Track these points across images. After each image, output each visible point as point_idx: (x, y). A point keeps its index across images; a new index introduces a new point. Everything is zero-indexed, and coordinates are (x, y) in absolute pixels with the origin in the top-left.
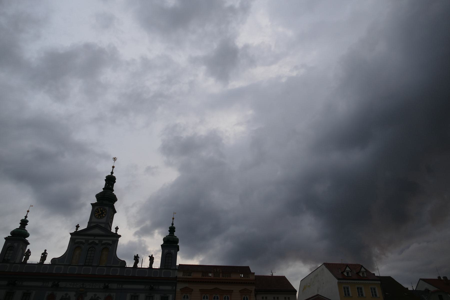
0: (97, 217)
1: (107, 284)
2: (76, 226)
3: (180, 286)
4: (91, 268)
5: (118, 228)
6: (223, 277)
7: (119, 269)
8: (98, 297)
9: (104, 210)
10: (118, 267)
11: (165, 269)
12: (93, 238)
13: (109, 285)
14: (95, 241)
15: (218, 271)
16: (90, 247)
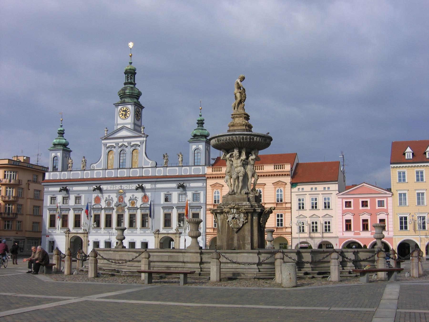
0: (122, 117)
3: (210, 182)
4: (125, 170)
7: (150, 169)
8: (136, 197)
9: (128, 109)
11: (194, 166)
12: (121, 140)
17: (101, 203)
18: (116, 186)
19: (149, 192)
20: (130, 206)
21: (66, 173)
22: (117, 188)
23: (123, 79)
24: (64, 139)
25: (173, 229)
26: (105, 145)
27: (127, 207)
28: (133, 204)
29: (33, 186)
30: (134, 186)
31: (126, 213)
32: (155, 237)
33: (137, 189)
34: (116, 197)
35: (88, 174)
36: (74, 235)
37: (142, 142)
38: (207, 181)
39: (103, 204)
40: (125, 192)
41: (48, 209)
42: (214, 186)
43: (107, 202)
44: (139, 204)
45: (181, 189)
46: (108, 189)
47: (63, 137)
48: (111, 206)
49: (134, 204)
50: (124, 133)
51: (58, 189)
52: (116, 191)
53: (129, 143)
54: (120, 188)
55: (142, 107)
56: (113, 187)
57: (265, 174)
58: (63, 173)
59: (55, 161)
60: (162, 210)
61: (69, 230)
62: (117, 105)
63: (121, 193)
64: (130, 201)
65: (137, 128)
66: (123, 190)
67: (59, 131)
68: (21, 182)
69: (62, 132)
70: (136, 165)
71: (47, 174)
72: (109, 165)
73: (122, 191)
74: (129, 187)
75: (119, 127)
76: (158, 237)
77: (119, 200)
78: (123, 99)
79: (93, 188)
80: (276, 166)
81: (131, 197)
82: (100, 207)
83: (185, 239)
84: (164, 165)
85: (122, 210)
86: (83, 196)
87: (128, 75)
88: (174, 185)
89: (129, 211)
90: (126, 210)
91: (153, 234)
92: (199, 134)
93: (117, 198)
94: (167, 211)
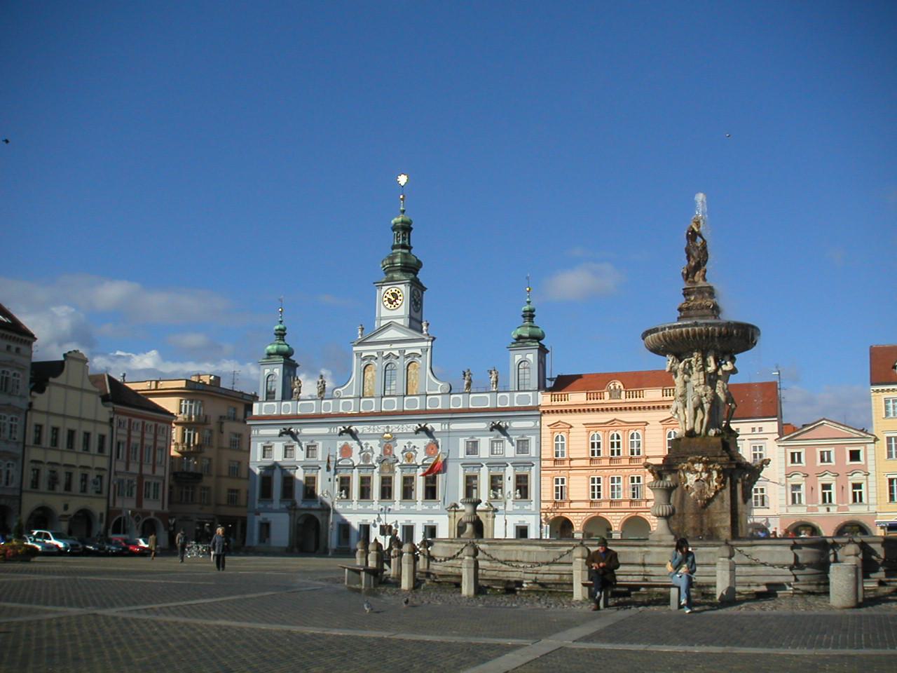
1: (423, 425)
3: (548, 420)
4: (395, 399)
6: (628, 398)
7: (439, 397)
8: (415, 447)
10: (439, 394)
11: (519, 391)
12: (388, 346)
14: (393, 352)
15: (617, 387)
16: (387, 365)
17: (351, 456)
18: (379, 426)
20: (404, 463)
21: (289, 403)
22: (381, 431)
23: (392, 238)
24: (286, 344)
26: (359, 354)
27: (399, 464)
28: (409, 458)
29: (230, 427)
30: (413, 427)
31: (396, 474)
32: (450, 517)
33: (417, 432)
34: (380, 446)
35: (328, 406)
36: (303, 513)
37: (424, 350)
38: (542, 418)
39: (356, 459)
40: (394, 438)
41: (259, 467)
42: (554, 425)
43: (364, 455)
44: (420, 458)
45: (496, 432)
46: (365, 432)
47: (284, 340)
50: (391, 334)
51: (277, 431)
52: (379, 437)
53: (402, 351)
54: (386, 430)
55: (424, 289)
57: (647, 405)
58: (284, 403)
59: (269, 383)
60: (461, 469)
61: (294, 504)
62: (380, 284)
63: (389, 438)
64: (404, 454)
65: (414, 323)
66: (391, 434)
67: (277, 330)
68: (208, 419)
69: (282, 332)
70: (414, 390)
71: (256, 406)
72: (367, 390)
73: (389, 435)
75: (383, 323)
76: (455, 517)
77: (385, 451)
78: (390, 275)
79: (338, 430)
80: (666, 390)
81: (405, 447)
82: (351, 463)
83: (506, 521)
84: (464, 390)
86: (320, 444)
87: (398, 232)
88: (483, 425)
89: (402, 471)
91: (446, 512)
92: (526, 335)
94: (470, 472)
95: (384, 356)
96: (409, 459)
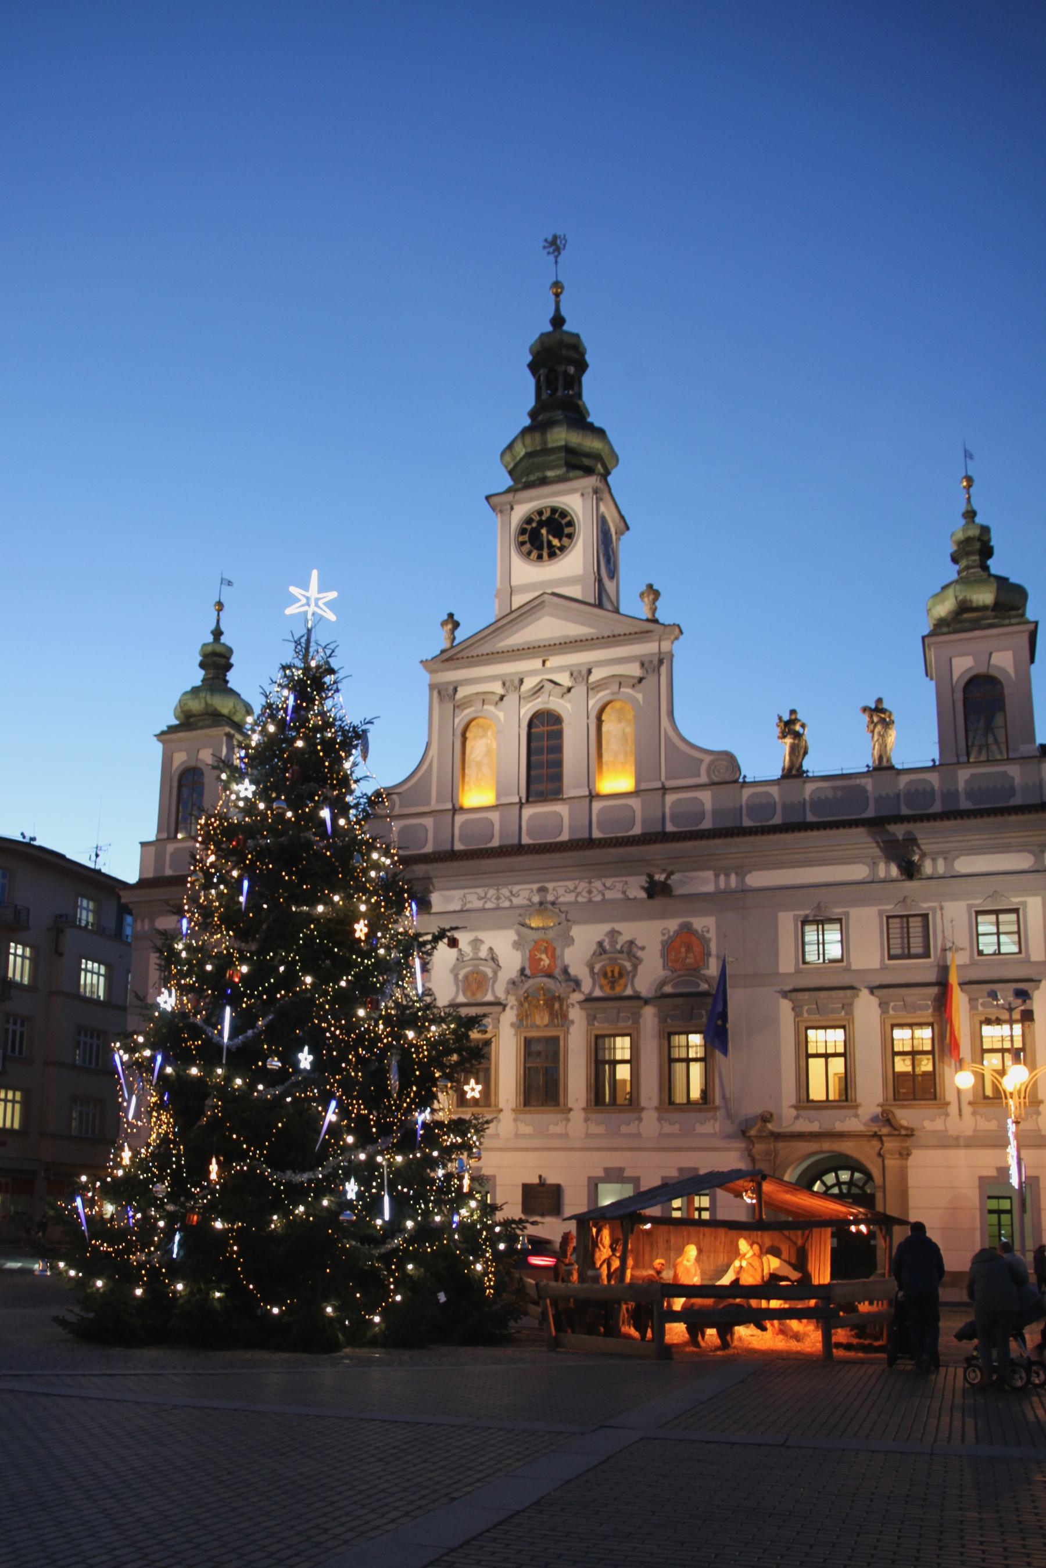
2: (444, 624)
5: (657, 594)
8: (631, 943)
12: (537, 663)
13: (669, 882)
18: (516, 888)
19: (702, 913)
20: (598, 993)
25: (860, 1111)
27: (576, 997)
31: (572, 1029)
34: (517, 945)
46: (469, 906)
48: (486, 994)
49: (622, 982)
54: (536, 899)
56: (498, 898)
74: (590, 892)
85: (553, 1015)
89: (591, 1019)
90: (576, 1014)
93: (523, 957)
95: (524, 688)
96: (613, 984)
